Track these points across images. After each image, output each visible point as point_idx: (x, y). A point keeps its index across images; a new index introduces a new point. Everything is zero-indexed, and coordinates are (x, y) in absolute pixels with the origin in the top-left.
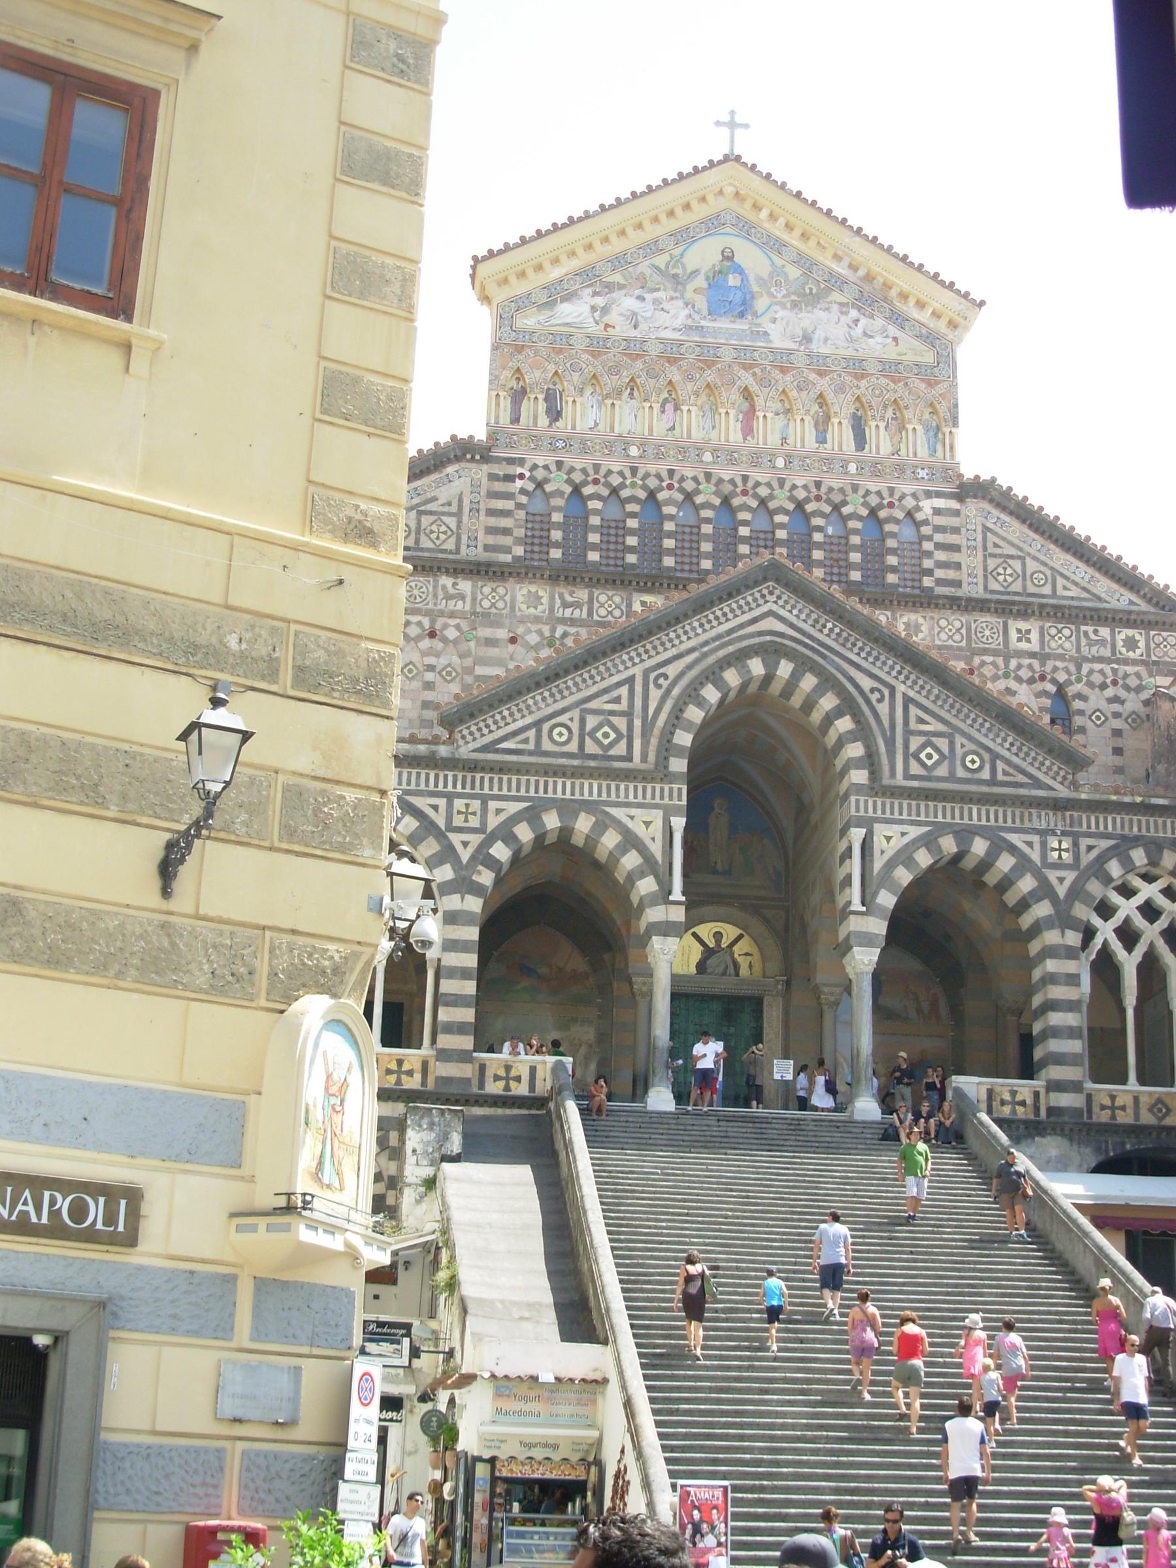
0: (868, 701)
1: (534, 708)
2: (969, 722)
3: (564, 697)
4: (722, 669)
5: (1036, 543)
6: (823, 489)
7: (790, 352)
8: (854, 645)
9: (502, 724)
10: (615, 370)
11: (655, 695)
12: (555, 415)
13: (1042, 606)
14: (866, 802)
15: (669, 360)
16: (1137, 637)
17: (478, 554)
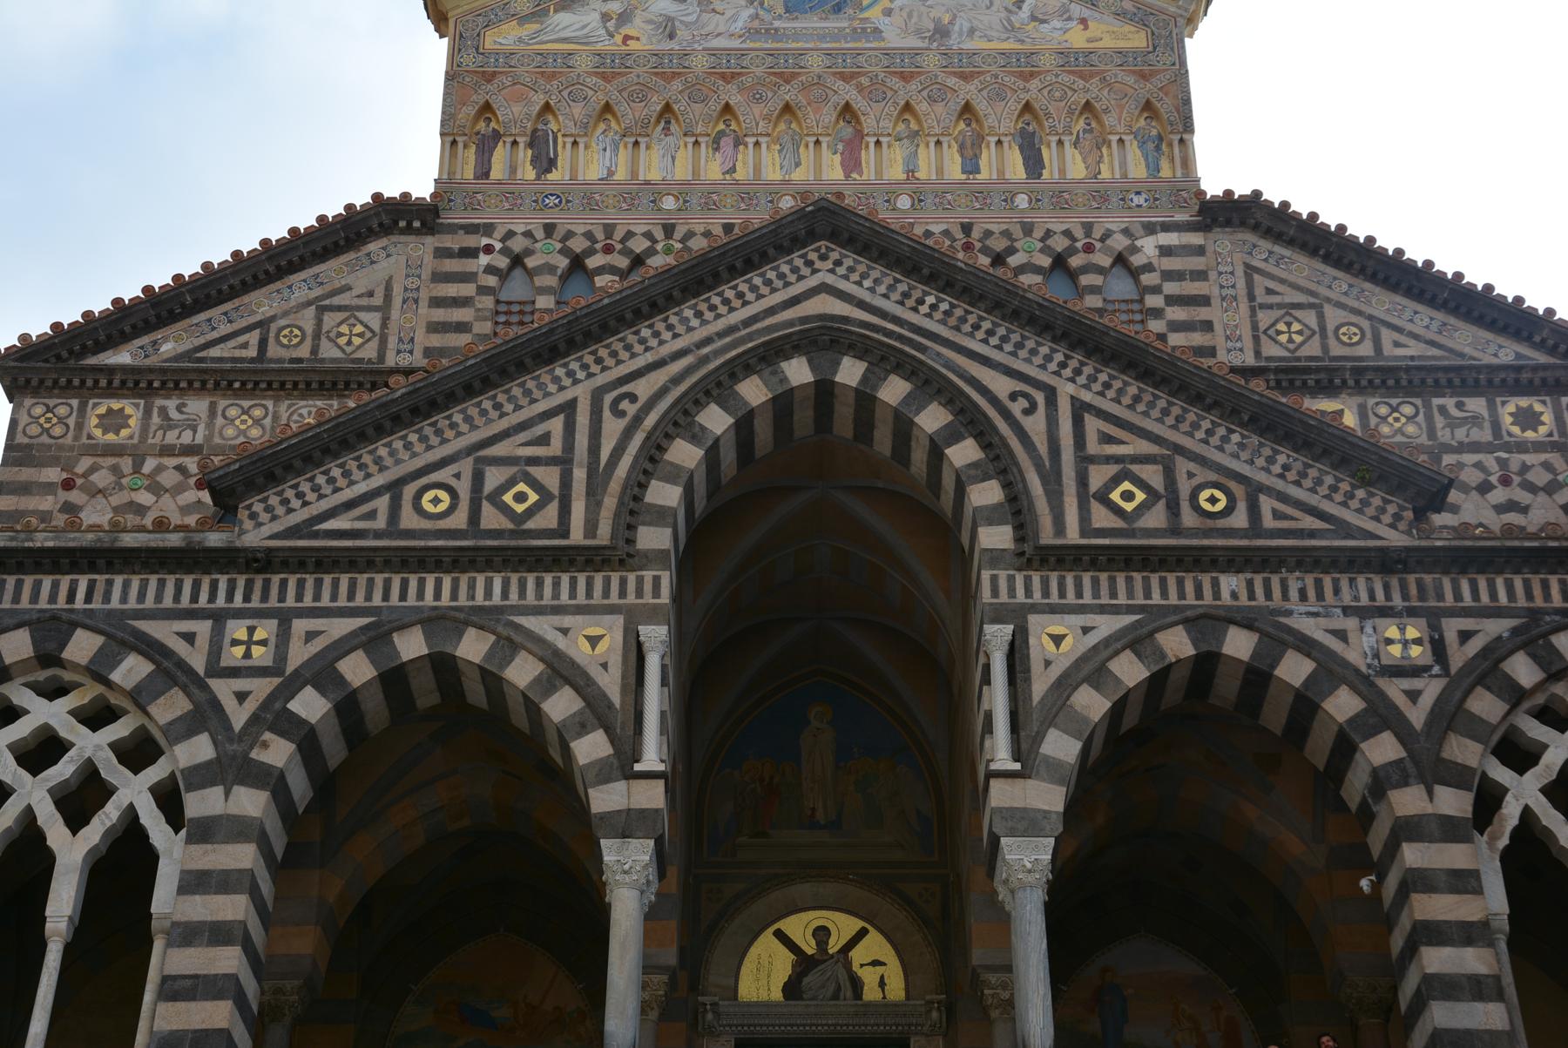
0: (1007, 415)
1: (388, 461)
2: (1200, 435)
3: (444, 441)
4: (734, 377)
5: (1338, 284)
6: (976, 234)
7: (916, 53)
8: (976, 327)
9: (327, 490)
10: (641, 94)
11: (612, 427)
12: (545, 164)
13: (1358, 372)
14: (1011, 579)
15: (723, 76)
16: (1538, 407)
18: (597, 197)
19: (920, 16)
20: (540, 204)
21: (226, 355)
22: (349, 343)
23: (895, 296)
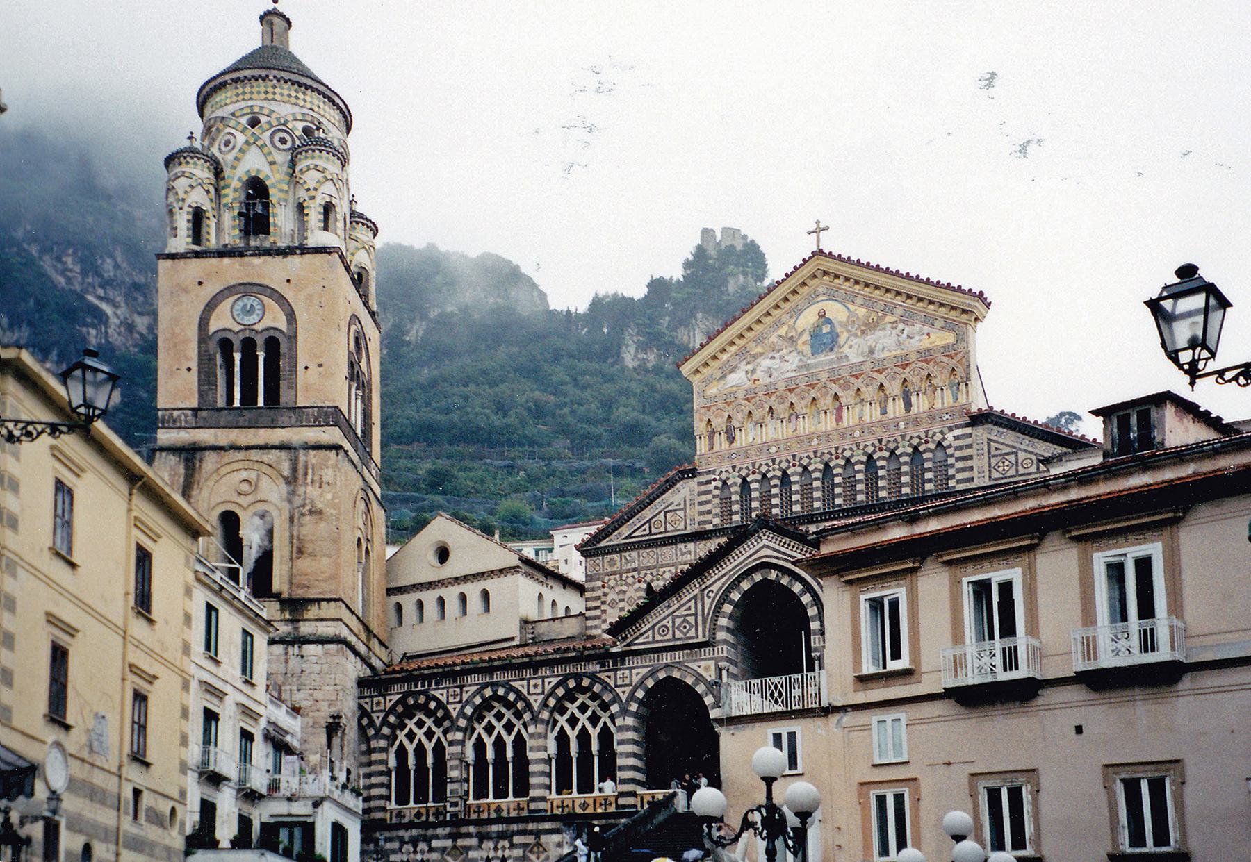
7: (861, 364)
12: (732, 439)
17: (696, 528)
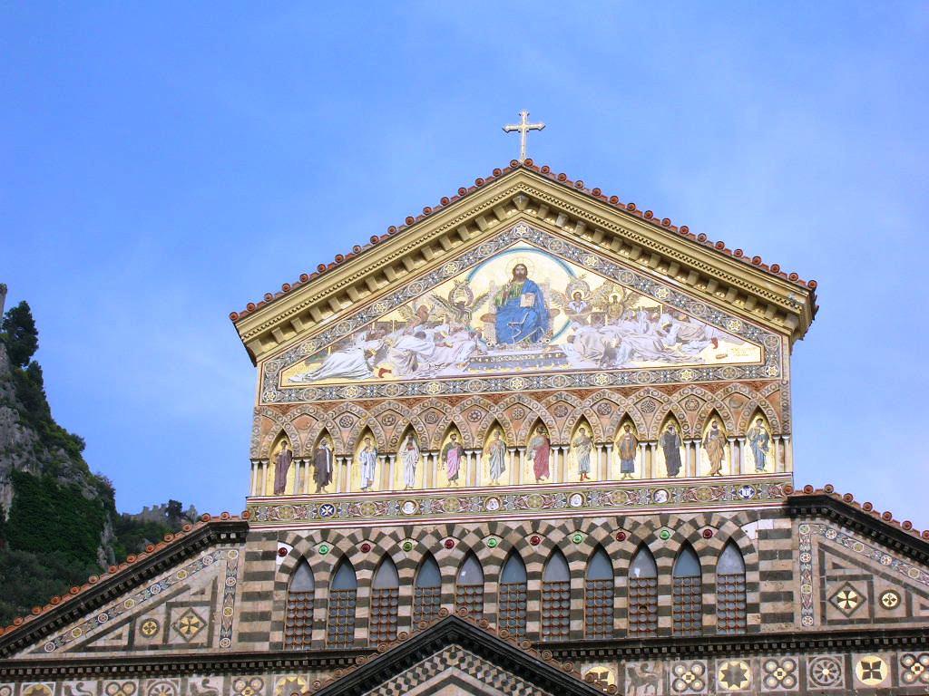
5: (886, 559)
6: (627, 525)
7: (590, 373)
12: (323, 478)
17: (235, 646)
18: (358, 505)
19: (595, 341)
20: (319, 517)
21: (107, 645)
22: (188, 632)
23: (498, 684)
